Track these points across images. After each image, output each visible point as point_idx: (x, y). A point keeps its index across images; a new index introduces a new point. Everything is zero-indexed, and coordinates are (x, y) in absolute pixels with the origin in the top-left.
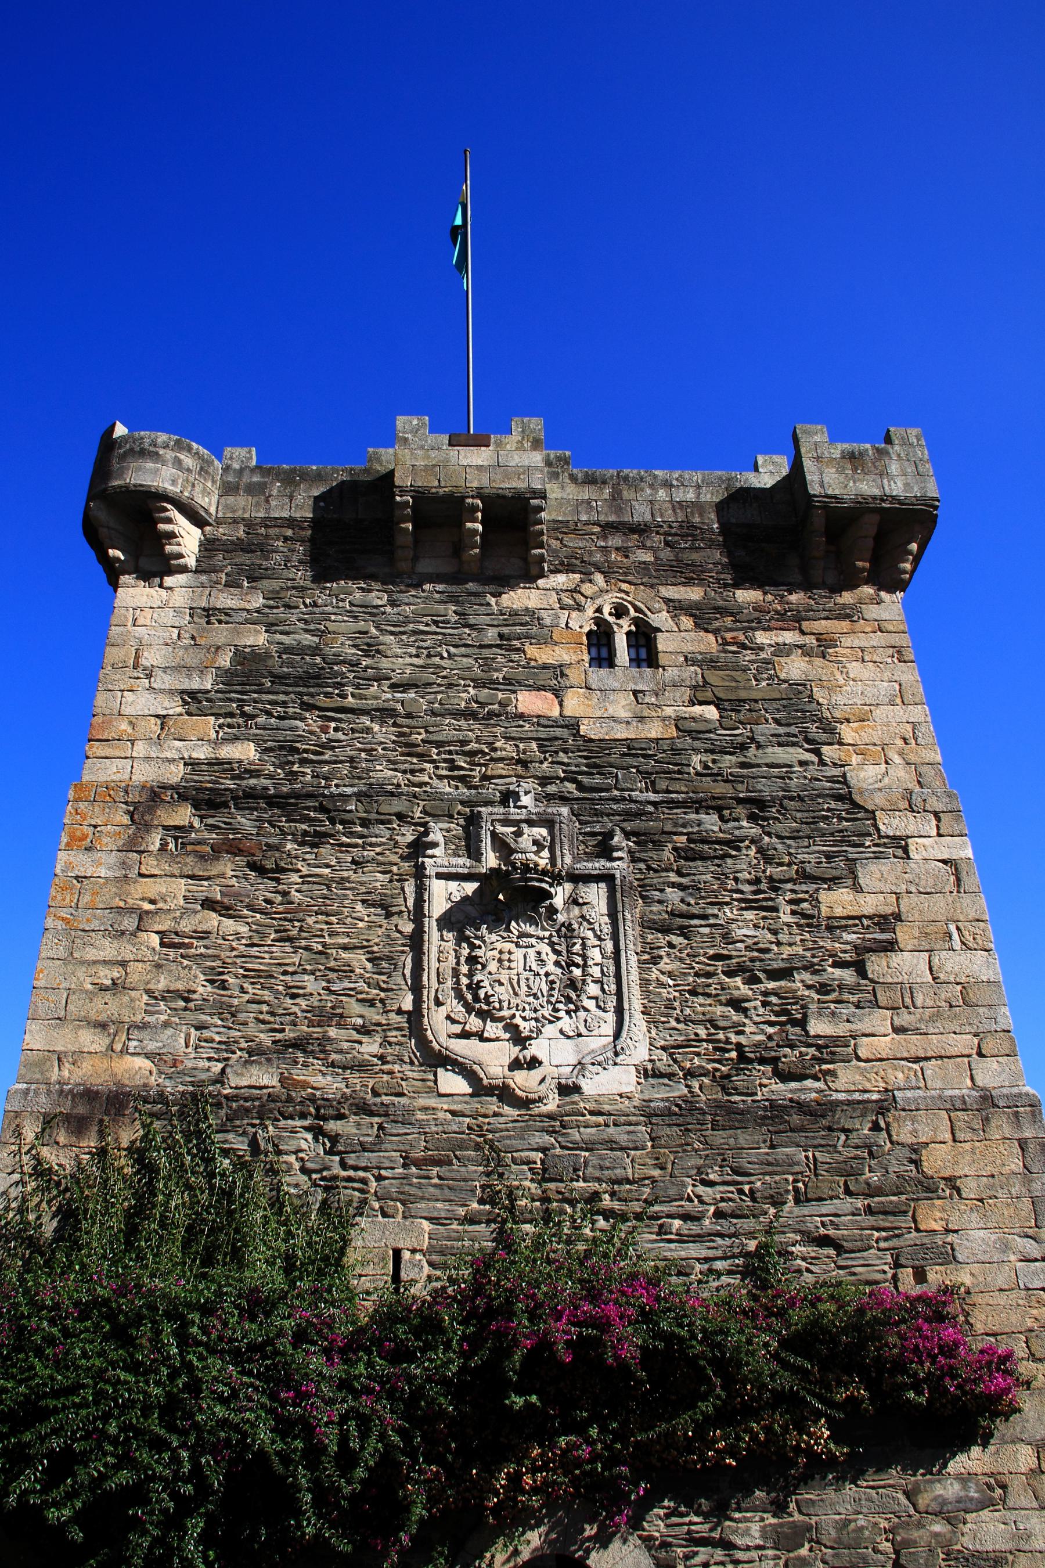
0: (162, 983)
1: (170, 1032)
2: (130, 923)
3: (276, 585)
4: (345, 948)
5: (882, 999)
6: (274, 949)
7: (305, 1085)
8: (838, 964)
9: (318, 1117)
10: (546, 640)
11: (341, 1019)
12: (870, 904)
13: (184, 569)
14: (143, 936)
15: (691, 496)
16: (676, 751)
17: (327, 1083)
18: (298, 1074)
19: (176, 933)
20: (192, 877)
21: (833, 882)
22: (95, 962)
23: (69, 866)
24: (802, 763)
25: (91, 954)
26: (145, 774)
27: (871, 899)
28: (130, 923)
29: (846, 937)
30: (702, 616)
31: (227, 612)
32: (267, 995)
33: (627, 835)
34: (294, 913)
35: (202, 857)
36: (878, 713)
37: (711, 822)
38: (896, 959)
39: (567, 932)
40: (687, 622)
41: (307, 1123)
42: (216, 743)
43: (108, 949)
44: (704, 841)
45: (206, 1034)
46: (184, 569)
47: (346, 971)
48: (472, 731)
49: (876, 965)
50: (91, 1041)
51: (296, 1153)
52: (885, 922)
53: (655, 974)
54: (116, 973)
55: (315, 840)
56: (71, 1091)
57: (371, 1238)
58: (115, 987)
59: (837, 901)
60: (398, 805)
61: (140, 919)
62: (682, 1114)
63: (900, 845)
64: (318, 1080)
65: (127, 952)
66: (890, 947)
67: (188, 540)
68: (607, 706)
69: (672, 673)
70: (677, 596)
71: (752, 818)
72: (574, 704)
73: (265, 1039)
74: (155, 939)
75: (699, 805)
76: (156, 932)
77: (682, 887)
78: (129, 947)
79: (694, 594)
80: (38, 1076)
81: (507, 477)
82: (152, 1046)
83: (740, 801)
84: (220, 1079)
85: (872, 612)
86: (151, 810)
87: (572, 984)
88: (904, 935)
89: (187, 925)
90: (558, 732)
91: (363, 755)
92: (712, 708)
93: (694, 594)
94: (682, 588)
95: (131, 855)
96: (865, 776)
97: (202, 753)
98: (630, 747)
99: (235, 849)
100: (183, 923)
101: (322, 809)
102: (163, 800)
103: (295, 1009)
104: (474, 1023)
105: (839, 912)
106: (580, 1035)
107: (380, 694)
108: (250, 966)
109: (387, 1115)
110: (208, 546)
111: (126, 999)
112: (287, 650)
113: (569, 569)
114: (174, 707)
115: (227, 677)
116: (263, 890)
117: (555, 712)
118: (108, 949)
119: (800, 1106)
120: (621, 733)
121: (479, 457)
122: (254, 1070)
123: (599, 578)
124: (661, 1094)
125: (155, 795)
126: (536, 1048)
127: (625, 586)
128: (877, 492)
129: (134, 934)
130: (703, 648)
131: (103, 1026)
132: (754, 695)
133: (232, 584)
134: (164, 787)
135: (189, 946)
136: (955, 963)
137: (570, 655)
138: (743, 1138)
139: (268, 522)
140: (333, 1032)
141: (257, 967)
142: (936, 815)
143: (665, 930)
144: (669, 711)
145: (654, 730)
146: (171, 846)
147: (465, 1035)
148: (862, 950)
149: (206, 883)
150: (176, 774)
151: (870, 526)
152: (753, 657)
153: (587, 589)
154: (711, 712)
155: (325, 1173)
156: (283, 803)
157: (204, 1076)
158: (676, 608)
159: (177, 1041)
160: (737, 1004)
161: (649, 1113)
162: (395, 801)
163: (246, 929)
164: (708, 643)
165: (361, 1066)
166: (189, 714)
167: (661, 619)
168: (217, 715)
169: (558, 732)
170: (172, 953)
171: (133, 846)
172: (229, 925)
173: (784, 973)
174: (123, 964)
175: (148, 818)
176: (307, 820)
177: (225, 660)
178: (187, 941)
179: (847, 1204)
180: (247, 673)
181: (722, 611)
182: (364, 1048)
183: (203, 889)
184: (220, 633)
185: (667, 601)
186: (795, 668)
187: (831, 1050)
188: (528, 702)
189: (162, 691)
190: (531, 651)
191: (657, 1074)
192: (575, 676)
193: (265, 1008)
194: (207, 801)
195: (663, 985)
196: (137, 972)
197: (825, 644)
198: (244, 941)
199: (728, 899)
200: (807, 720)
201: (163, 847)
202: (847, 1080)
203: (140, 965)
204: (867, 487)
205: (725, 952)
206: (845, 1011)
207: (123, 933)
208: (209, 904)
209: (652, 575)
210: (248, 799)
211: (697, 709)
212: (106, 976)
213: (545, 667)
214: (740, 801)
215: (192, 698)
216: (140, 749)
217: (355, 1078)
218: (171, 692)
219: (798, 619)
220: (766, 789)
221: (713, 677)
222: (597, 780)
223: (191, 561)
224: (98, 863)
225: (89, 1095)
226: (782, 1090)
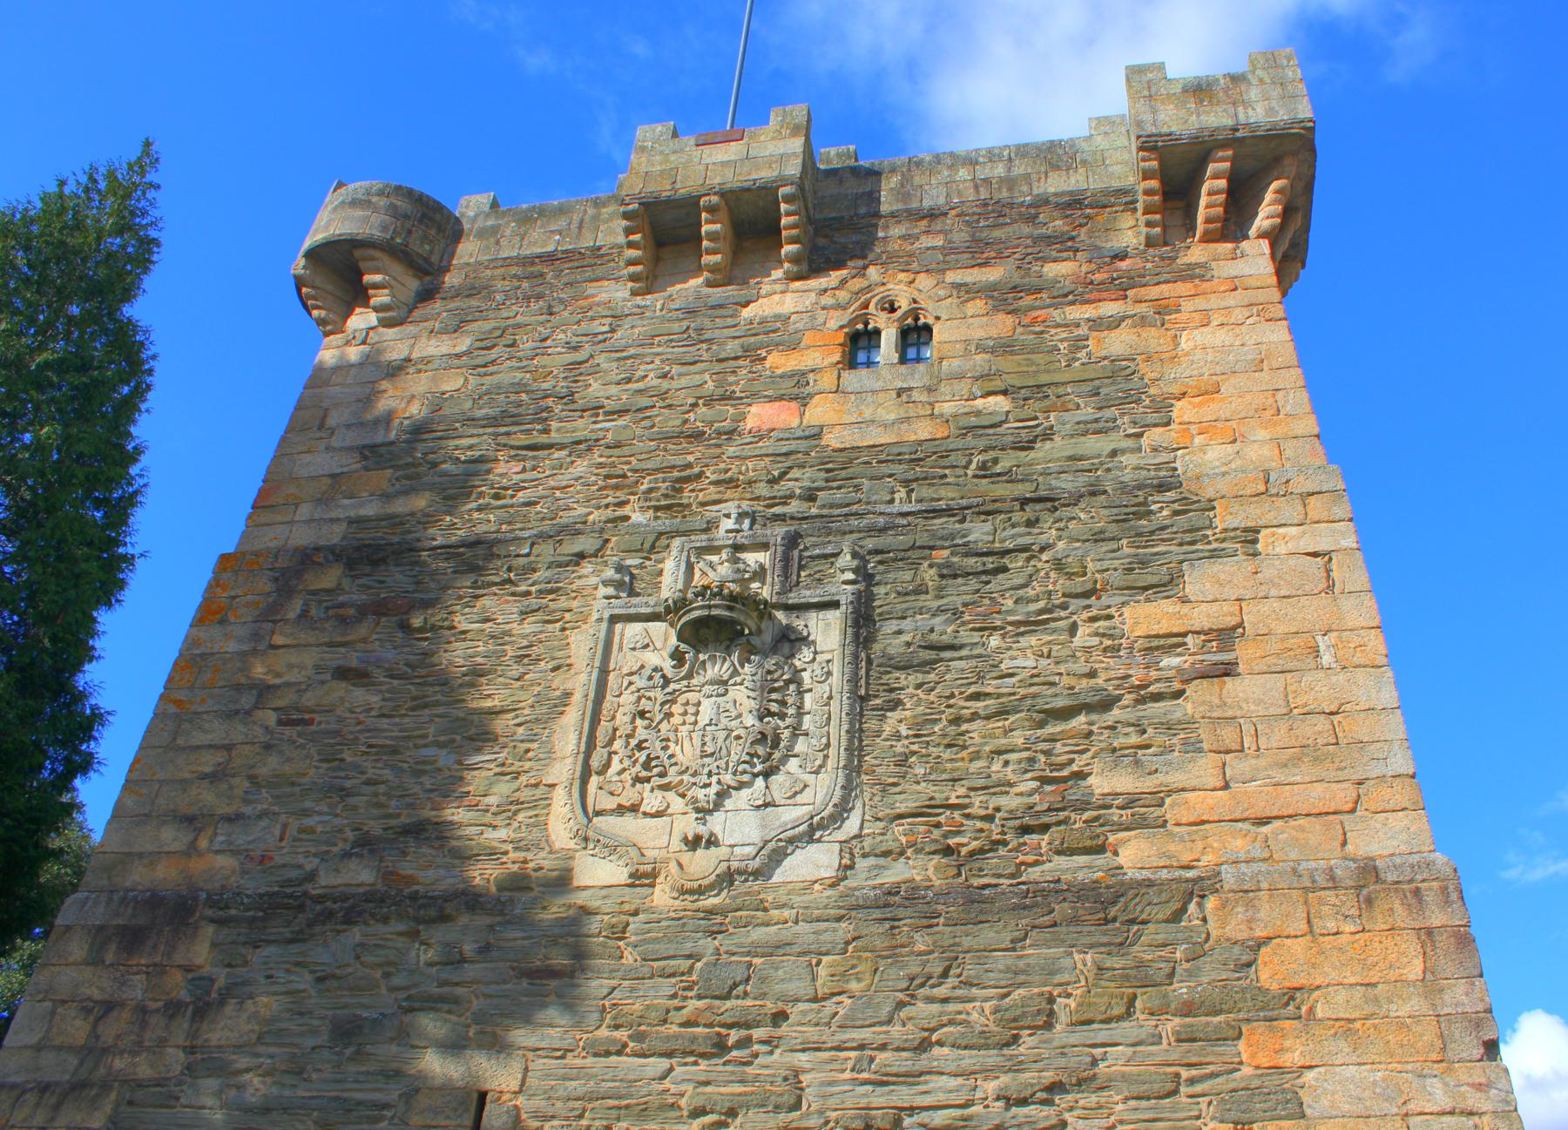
1: (264, 823)
2: (247, 701)
6: (407, 720)
7: (411, 880)
9: (418, 920)
14: (259, 714)
18: (407, 868)
19: (297, 709)
20: (331, 645)
22: (198, 747)
25: (199, 738)
28: (247, 701)
29: (1169, 661)
30: (1002, 298)
32: (387, 774)
35: (343, 621)
37: (978, 532)
41: (402, 927)
42: (387, 497)
43: (216, 731)
44: (966, 555)
45: (309, 822)
50: (171, 837)
51: (380, 965)
52: (1226, 636)
54: (220, 757)
56: (135, 897)
60: (585, 543)
61: (260, 695)
62: (892, 904)
65: (238, 732)
68: (862, 412)
70: (968, 279)
72: (819, 412)
73: (375, 828)
74: (271, 718)
76: (274, 709)
78: (241, 728)
80: (105, 882)
81: (758, 168)
82: (241, 840)
84: (312, 876)
86: (299, 574)
89: (309, 699)
91: (558, 494)
92: (1000, 398)
93: (993, 274)
94: (976, 270)
95: (264, 625)
97: (370, 510)
100: (309, 695)
102: (314, 563)
103: (417, 789)
106: (766, 805)
107: (583, 427)
108: (373, 741)
109: (502, 913)
111: (225, 786)
114: (350, 463)
117: (795, 423)
118: (216, 731)
122: (353, 864)
125: (307, 558)
127: (902, 276)
129: (248, 713)
130: (994, 333)
134: (317, 549)
135: (311, 722)
137: (819, 356)
138: (988, 935)
141: (380, 742)
146: (313, 612)
147: (621, 810)
149: (343, 650)
150: (334, 535)
152: (1064, 335)
154: (1000, 404)
155: (412, 992)
157: (294, 874)
161: (851, 908)
162: (582, 538)
163: (375, 699)
164: (1003, 325)
166: (367, 469)
168: (396, 467)
170: (288, 732)
172: (360, 696)
174: (229, 748)
175: (294, 582)
178: (307, 716)
182: (490, 834)
183: (339, 658)
185: (958, 286)
186: (1118, 342)
189: (341, 449)
193: (382, 788)
195: (897, 736)
197: (1164, 309)
198: (373, 713)
199: (999, 623)
200: (1123, 391)
201: (304, 614)
203: (247, 747)
205: (989, 690)
207: (237, 712)
208: (343, 674)
211: (979, 403)
216: (304, 511)
218: (351, 449)
220: (1067, 484)
221: (1005, 363)
222: (838, 496)
224: (227, 636)
225: (153, 901)
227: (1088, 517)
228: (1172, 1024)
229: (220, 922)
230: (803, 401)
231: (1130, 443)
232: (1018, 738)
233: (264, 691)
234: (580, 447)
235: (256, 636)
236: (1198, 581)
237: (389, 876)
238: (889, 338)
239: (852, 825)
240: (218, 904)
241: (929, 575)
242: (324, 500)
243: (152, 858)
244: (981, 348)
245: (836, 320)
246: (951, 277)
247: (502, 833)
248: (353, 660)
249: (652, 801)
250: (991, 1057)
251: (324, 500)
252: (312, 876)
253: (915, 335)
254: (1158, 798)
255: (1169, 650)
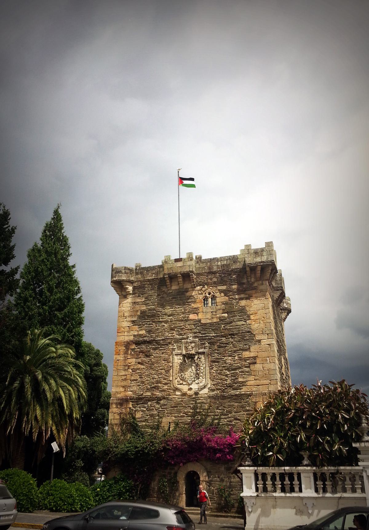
0: (133, 378)
2: (127, 368)
3: (146, 295)
4: (161, 369)
5: (253, 374)
8: (245, 367)
10: (195, 302)
11: (160, 382)
12: (252, 354)
13: (130, 294)
15: (225, 262)
16: (219, 324)
17: (158, 394)
18: (155, 393)
21: (246, 350)
23: (116, 358)
24: (243, 325)
25: (121, 374)
26: (127, 339)
27: (252, 353)
28: (127, 368)
30: (226, 293)
31: (138, 303)
33: (209, 343)
34: (153, 364)
36: (259, 312)
38: (256, 365)
39: (197, 365)
40: (222, 294)
43: (123, 373)
46: (130, 294)
47: (161, 374)
48: (182, 324)
49: (252, 367)
52: (255, 358)
53: (212, 371)
55: (155, 349)
57: (165, 421)
58: (125, 380)
59: (246, 354)
60: (169, 341)
63: (259, 341)
64: (158, 394)
66: (255, 363)
67: (130, 288)
68: (205, 315)
69: (219, 307)
71: (232, 338)
72: (200, 316)
75: (222, 336)
77: (218, 353)
79: (224, 287)
82: (132, 390)
83: (230, 335)
85: (261, 287)
87: (197, 374)
88: (258, 361)
90: (197, 322)
93: (224, 287)
96: (255, 326)
97: (136, 334)
98: (211, 324)
99: (142, 352)
101: (156, 343)
104: (181, 382)
105: (246, 356)
107: (166, 318)
110: (134, 288)
112: (150, 310)
113: (200, 285)
115: (140, 317)
116: (146, 360)
118: (123, 373)
119: (236, 395)
120: (209, 321)
121: (179, 264)
123: (206, 286)
124: (212, 393)
126: (191, 386)
128: (260, 261)
131: (123, 387)
132: (234, 310)
133: (139, 296)
136: (267, 366)
139: (145, 281)
140: (159, 385)
142: (268, 334)
143: (214, 362)
144: (218, 316)
145: (215, 320)
147: (181, 384)
148: (250, 364)
150: (132, 338)
151: (259, 268)
153: (204, 289)
154: (226, 315)
156: (149, 342)
158: (221, 291)
159: (135, 388)
160: (226, 376)
161: (209, 397)
165: (164, 391)
167: (218, 295)
169: (197, 322)
171: (126, 353)
173: (235, 369)
176: (154, 345)
177: (139, 313)
179: (242, 413)
180: (143, 315)
181: (230, 291)
184: (138, 307)
185: (219, 290)
187: (243, 384)
188: (192, 316)
190: (193, 305)
191: (212, 390)
192: (201, 310)
194: (137, 343)
196: (128, 377)
202: (244, 390)
204: (258, 260)
206: (245, 376)
208: (139, 363)
209: (216, 284)
210: (145, 342)
211: (223, 315)
212: (124, 377)
213: (195, 308)
214: (230, 335)
215: (133, 322)
217: (163, 393)
218: (130, 321)
219: (245, 291)
223: (131, 292)
225: (122, 399)
226: (233, 392)
227: (237, 338)
228: (245, 413)
229: (132, 402)
230: (197, 314)
231: (244, 323)
232: (228, 373)
233: (129, 367)
234: (166, 322)
235: (125, 357)
236: (252, 349)
237: (152, 394)
238: (210, 300)
239: (209, 386)
240: (131, 399)
241: (216, 347)
242: (128, 332)
243: (121, 392)
244: (223, 304)
245: (201, 297)
246: (220, 288)
247: (166, 387)
248: (140, 360)
249: (184, 383)
250: (226, 417)
251: (128, 332)
252: (142, 395)
253: (214, 298)
254: (245, 382)
255: (248, 360)
